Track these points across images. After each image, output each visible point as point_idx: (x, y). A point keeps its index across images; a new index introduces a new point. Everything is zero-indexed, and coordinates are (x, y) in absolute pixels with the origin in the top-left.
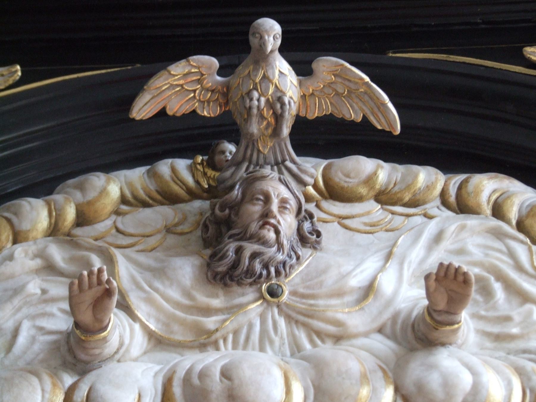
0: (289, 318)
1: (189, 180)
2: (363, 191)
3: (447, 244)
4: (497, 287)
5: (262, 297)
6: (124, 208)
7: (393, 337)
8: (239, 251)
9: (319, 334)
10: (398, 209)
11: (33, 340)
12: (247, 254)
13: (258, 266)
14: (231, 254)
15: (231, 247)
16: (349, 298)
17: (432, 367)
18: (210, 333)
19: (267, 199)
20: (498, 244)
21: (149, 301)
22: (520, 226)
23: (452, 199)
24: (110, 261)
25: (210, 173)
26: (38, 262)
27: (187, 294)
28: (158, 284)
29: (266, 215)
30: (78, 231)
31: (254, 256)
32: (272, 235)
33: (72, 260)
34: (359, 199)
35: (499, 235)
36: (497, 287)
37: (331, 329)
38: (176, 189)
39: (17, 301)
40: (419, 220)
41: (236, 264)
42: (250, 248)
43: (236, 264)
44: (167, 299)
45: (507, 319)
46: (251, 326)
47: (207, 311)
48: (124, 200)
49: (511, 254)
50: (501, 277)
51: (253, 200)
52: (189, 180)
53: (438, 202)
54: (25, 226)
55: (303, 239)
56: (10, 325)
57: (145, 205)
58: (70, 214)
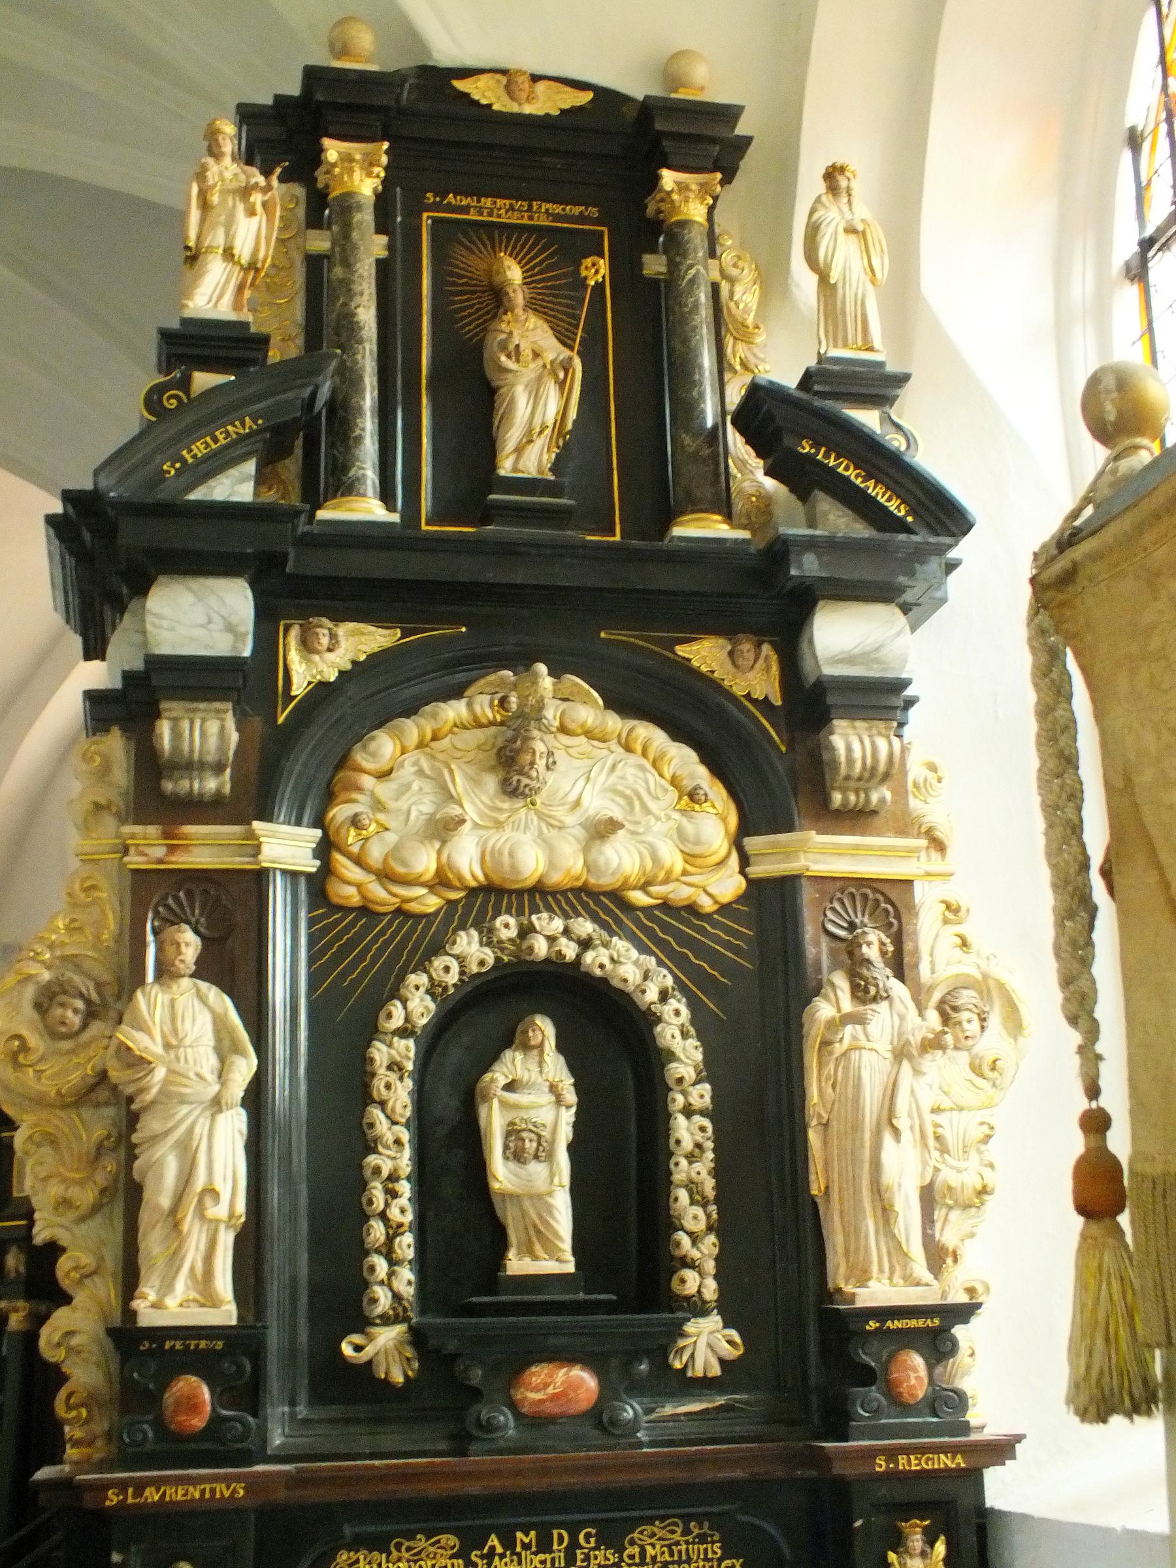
0: (539, 817)
1: (490, 716)
2: (579, 731)
3: (618, 772)
4: (637, 803)
5: (526, 805)
6: (456, 729)
7: (585, 828)
8: (519, 781)
9: (552, 825)
10: (596, 743)
11: (417, 818)
12: (522, 784)
13: (527, 791)
14: (515, 783)
15: (516, 778)
16: (567, 807)
17: (601, 853)
18: (502, 823)
19: (534, 753)
20: (641, 774)
21: (473, 803)
22: (654, 764)
23: (623, 741)
24: (451, 772)
25: (502, 712)
26: (416, 768)
27: (491, 800)
28: (477, 791)
29: (532, 763)
30: (434, 744)
31: (526, 786)
32: (534, 774)
33: (433, 768)
34: (578, 735)
35: (642, 768)
36: (637, 803)
37: (557, 824)
38: (484, 721)
39: (408, 794)
40: (605, 752)
41: (516, 789)
42: (525, 781)
43: (516, 789)
44: (481, 801)
45: (639, 823)
46: (520, 820)
47: (500, 810)
48: (455, 725)
49: (647, 782)
50: (640, 798)
51: (526, 752)
52: (490, 716)
53: (616, 740)
54: (407, 744)
55: (548, 768)
56: (405, 807)
57: (466, 728)
58: (429, 735)
